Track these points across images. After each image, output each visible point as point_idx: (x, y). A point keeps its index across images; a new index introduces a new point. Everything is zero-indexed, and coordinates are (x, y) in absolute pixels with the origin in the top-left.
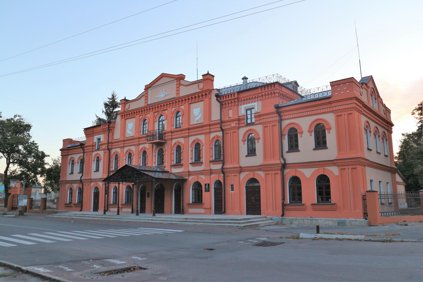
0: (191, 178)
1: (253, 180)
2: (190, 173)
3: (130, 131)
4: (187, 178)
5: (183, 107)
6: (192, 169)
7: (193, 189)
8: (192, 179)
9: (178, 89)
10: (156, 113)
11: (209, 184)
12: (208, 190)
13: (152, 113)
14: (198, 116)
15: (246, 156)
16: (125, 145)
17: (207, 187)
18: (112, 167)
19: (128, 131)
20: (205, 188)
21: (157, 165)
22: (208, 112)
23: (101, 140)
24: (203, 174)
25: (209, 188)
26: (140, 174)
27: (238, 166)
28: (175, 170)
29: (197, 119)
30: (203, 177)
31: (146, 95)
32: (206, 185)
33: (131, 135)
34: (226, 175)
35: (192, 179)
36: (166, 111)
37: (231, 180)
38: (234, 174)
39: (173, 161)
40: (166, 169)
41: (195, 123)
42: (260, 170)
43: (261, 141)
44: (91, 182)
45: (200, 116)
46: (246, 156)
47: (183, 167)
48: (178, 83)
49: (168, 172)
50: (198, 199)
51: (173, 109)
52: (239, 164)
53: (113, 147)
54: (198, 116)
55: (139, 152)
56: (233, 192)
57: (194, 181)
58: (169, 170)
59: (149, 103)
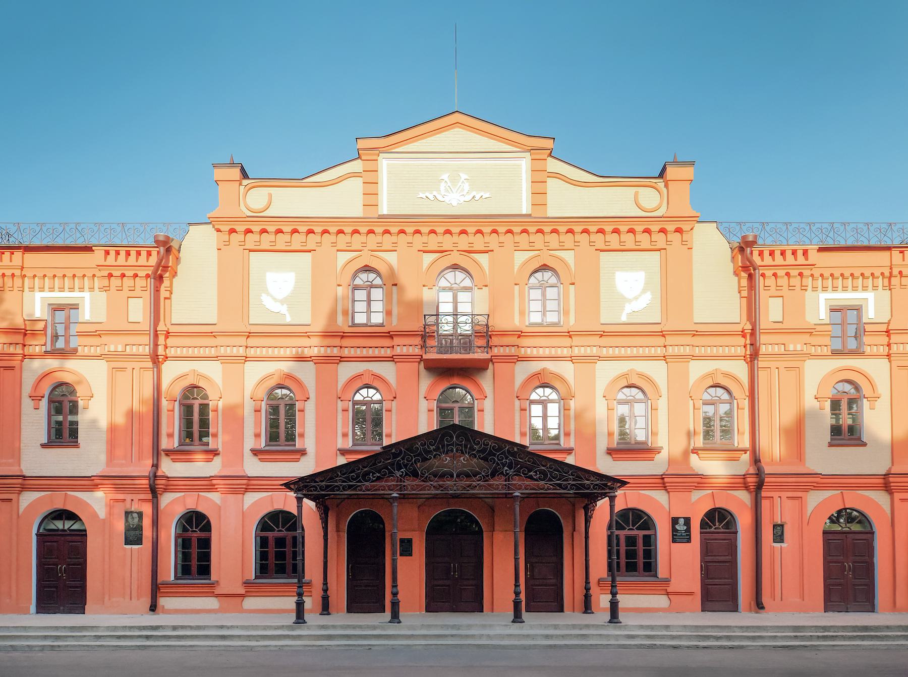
1: (844, 514)
3: (282, 302)
9: (539, 188)
10: (428, 258)
11: (687, 521)
14: (636, 298)
16: (252, 352)
17: (681, 527)
18: (170, 435)
19: (265, 298)
20: (674, 530)
22: (674, 287)
23: (86, 314)
29: (628, 308)
30: (660, 496)
31: (370, 177)
32: (675, 521)
33: (288, 320)
36: (483, 259)
38: (790, 494)
41: (624, 319)
43: (884, 403)
44: (24, 488)
45: (646, 299)
48: (539, 165)
53: (171, 352)
54: (636, 298)
56: (777, 545)
59: (384, 210)
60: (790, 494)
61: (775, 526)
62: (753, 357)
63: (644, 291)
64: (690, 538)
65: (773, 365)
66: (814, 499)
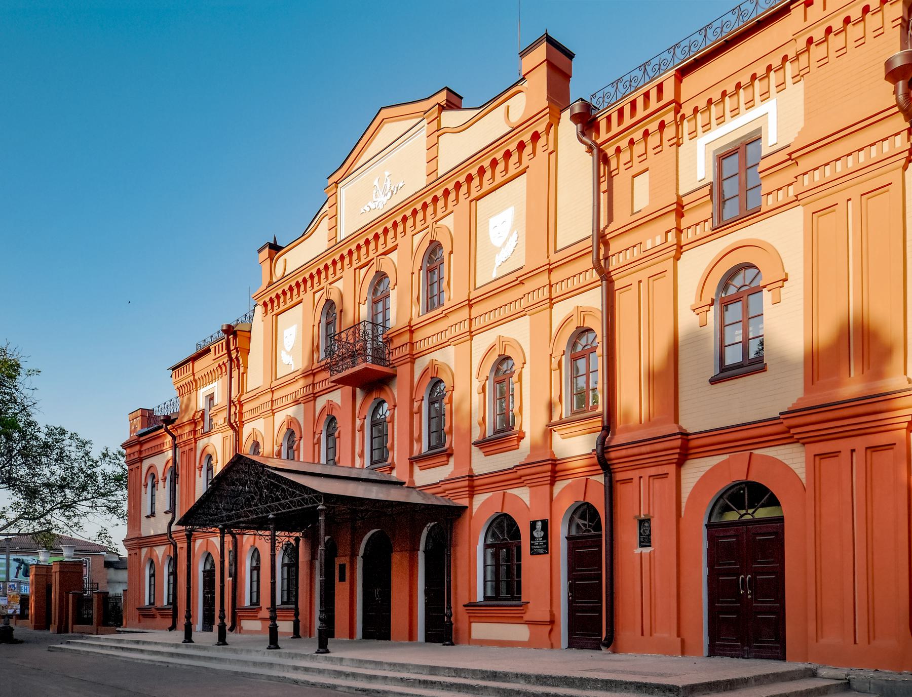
0: (479, 500)
2: (473, 484)
4: (464, 502)
5: (449, 222)
6: (482, 464)
7: (487, 546)
8: (482, 506)
10: (363, 271)
11: (545, 523)
12: (543, 547)
13: (348, 272)
14: (505, 244)
15: (714, 381)
17: (538, 534)
20: (533, 538)
21: (367, 462)
24: (521, 484)
25: (545, 537)
26: (277, 487)
27: (672, 429)
28: (424, 477)
29: (499, 259)
30: (523, 494)
32: (533, 525)
34: (619, 476)
35: (482, 506)
36: (394, 256)
37: (641, 496)
38: (653, 471)
39: (419, 439)
40: (394, 473)
42: (786, 437)
46: (714, 381)
47: (452, 460)
49: (402, 484)
50: (506, 591)
51: (417, 239)
52: (676, 420)
54: (505, 244)
55: (316, 422)
57: (489, 515)
58: (406, 479)
60: (653, 471)
61: (641, 522)
62: (606, 277)
63: (511, 234)
64: (547, 548)
65: (633, 279)
66: (694, 472)
